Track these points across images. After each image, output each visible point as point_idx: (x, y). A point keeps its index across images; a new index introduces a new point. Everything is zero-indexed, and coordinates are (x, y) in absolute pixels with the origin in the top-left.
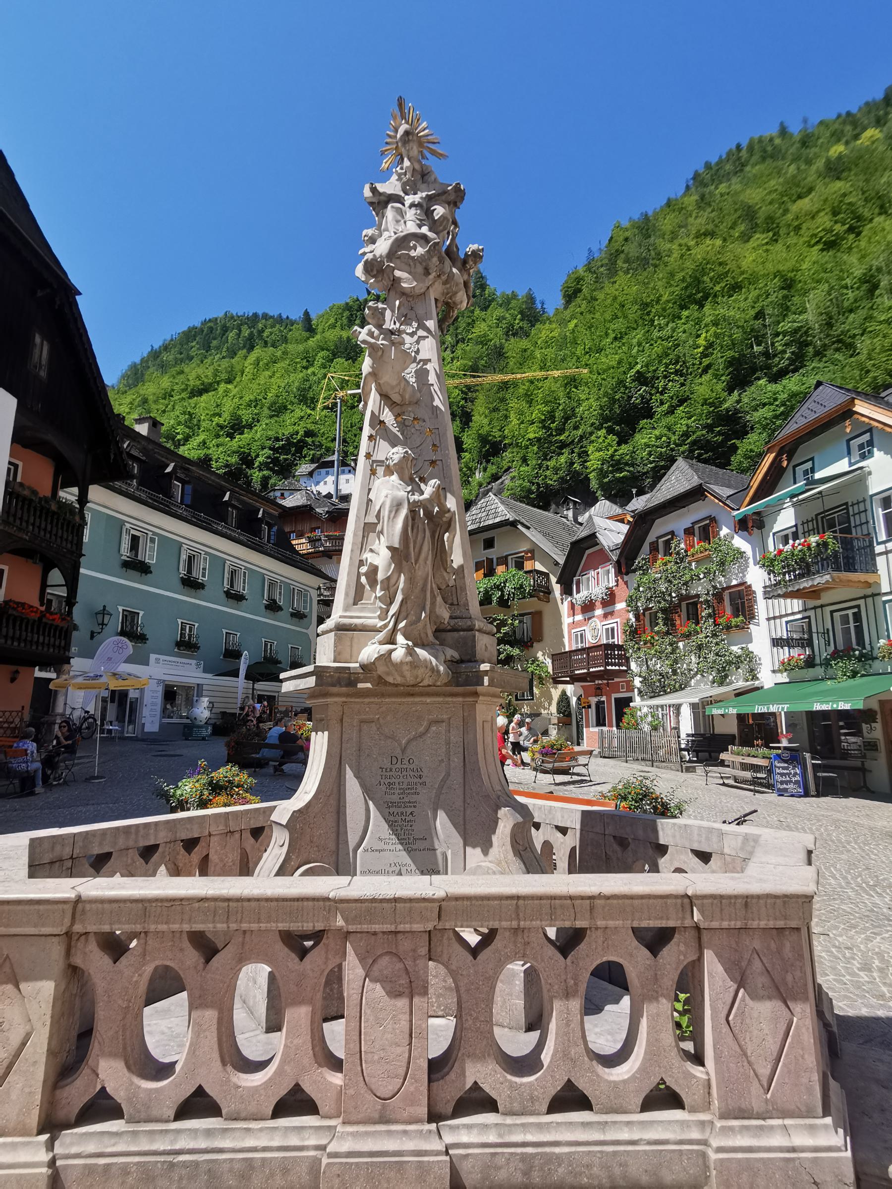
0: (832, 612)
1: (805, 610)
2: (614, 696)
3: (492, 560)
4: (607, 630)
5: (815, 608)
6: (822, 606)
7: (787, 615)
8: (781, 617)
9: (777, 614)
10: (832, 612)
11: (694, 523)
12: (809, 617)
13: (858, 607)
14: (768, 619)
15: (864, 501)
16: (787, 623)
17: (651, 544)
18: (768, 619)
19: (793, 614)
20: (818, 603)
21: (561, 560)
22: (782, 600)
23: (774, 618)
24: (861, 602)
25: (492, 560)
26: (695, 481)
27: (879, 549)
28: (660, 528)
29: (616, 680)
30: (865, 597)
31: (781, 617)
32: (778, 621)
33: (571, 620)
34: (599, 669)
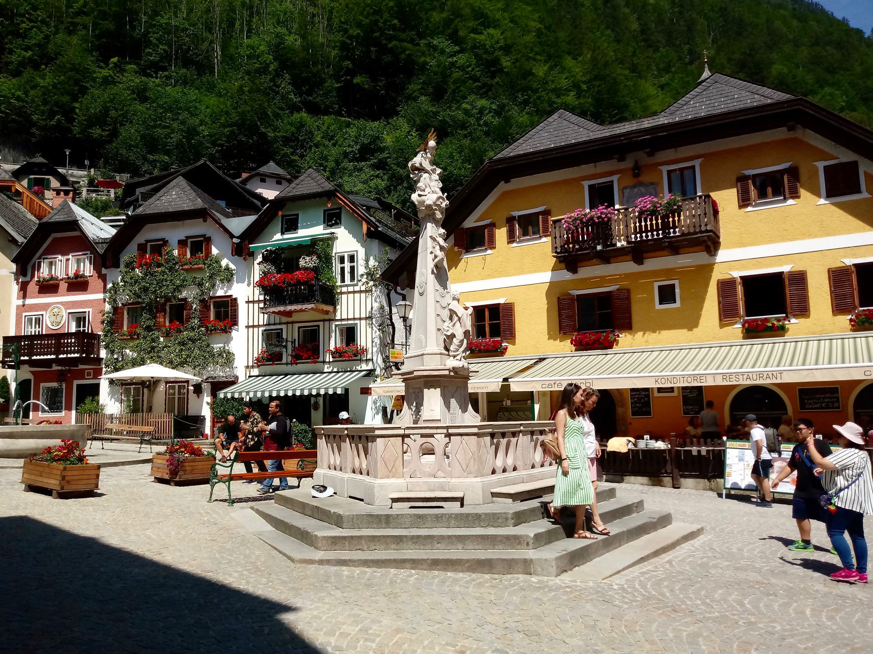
0: (299, 328)
1: (280, 324)
2: (76, 382)
5: (287, 323)
6: (293, 323)
9: (256, 323)
10: (299, 328)
11: (188, 238)
12: (282, 329)
13: (318, 326)
14: (248, 327)
18: (248, 327)
20: (290, 320)
23: (253, 326)
24: (321, 324)
26: (199, 203)
28: (150, 233)
29: (81, 367)
30: (324, 320)
32: (256, 329)
33: (20, 302)
34: (49, 357)
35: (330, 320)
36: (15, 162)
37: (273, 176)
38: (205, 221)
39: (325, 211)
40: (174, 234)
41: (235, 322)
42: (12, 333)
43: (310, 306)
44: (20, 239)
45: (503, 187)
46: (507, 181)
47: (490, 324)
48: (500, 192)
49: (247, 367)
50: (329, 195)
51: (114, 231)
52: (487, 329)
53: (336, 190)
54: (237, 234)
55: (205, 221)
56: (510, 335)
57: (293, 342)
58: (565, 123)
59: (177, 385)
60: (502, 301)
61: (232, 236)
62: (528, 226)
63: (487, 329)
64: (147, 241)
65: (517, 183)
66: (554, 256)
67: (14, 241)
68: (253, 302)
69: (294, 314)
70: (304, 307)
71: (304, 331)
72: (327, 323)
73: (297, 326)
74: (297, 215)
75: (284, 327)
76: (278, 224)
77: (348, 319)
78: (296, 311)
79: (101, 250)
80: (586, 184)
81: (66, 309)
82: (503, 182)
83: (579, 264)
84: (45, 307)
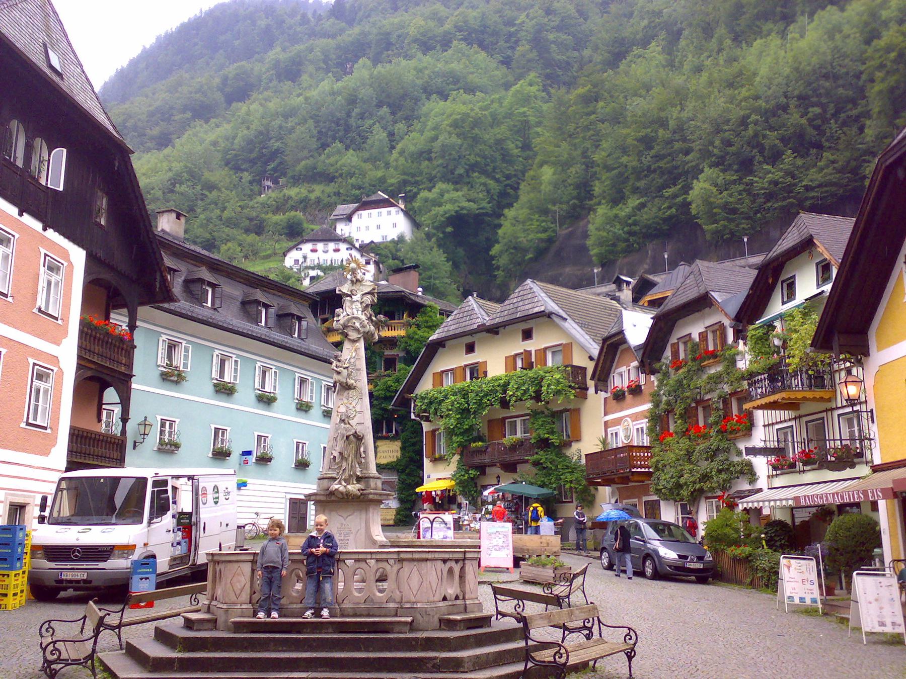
1: (790, 420)
2: (645, 499)
3: (530, 352)
4: (638, 429)
6: (800, 417)
7: (777, 423)
9: (774, 421)
12: (792, 426)
14: (765, 426)
16: (778, 430)
18: (765, 426)
21: (596, 358)
23: (769, 425)
24: (824, 414)
25: (530, 352)
30: (826, 411)
31: (773, 424)
32: (771, 428)
35: (832, 409)
73: (805, 419)
75: (792, 423)
78: (804, 398)
84: (618, 422)
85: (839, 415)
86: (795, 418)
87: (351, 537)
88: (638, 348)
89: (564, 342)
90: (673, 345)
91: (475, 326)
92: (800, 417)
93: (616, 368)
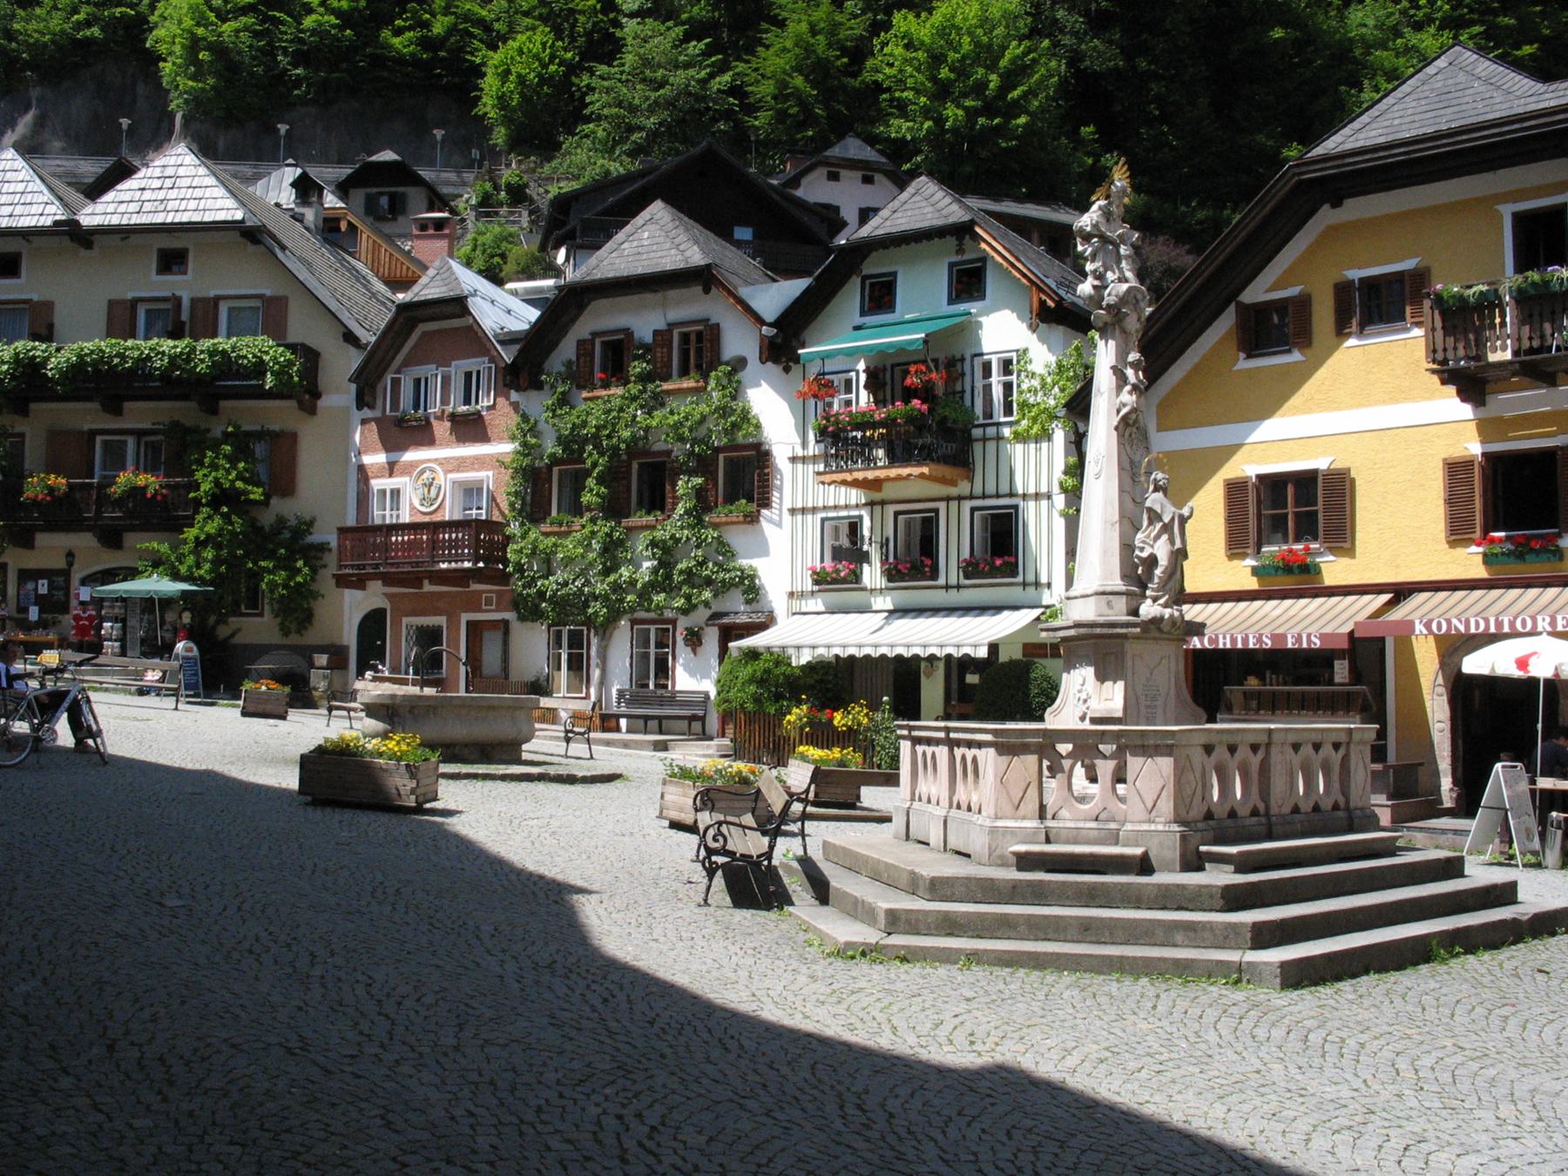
2: (465, 617)
6: (883, 503)
8: (814, 510)
10: (897, 514)
13: (936, 511)
14: (793, 511)
15: (963, 360)
16: (823, 520)
17: (581, 344)
19: (836, 507)
21: (368, 338)
22: (843, 489)
23: (804, 511)
24: (942, 506)
27: (977, 432)
30: (948, 499)
31: (814, 510)
35: (960, 498)
36: (341, 161)
37: (853, 164)
38: (707, 291)
39: (951, 265)
40: (645, 321)
41: (766, 503)
42: (351, 521)
43: (916, 471)
44: (368, 338)
45: (1326, 216)
46: (1337, 204)
47: (1296, 514)
48: (1322, 228)
49: (791, 594)
50: (963, 231)
51: (533, 314)
52: (1291, 524)
53: (972, 223)
54: (770, 315)
55: (707, 291)
56: (1341, 537)
57: (884, 544)
58: (1462, 77)
59: (653, 628)
60: (1321, 464)
61: (760, 321)
62: (1374, 305)
63: (1291, 524)
64: (595, 335)
65: (1357, 208)
66: (1434, 372)
67: (350, 338)
68: (804, 459)
69: (887, 486)
70: (905, 471)
71: (908, 524)
72: (954, 505)
74: (894, 274)
76: (850, 298)
77: (998, 496)
78: (888, 479)
79: (507, 355)
80: (1507, 211)
81: (447, 472)
82: (1326, 207)
83: (1488, 387)
85: (973, 510)
86: (871, 504)
87: (1159, 703)
88: (508, 339)
89: (268, 293)
90: (581, 343)
91: (48, 222)
92: (883, 503)
93: (407, 363)
